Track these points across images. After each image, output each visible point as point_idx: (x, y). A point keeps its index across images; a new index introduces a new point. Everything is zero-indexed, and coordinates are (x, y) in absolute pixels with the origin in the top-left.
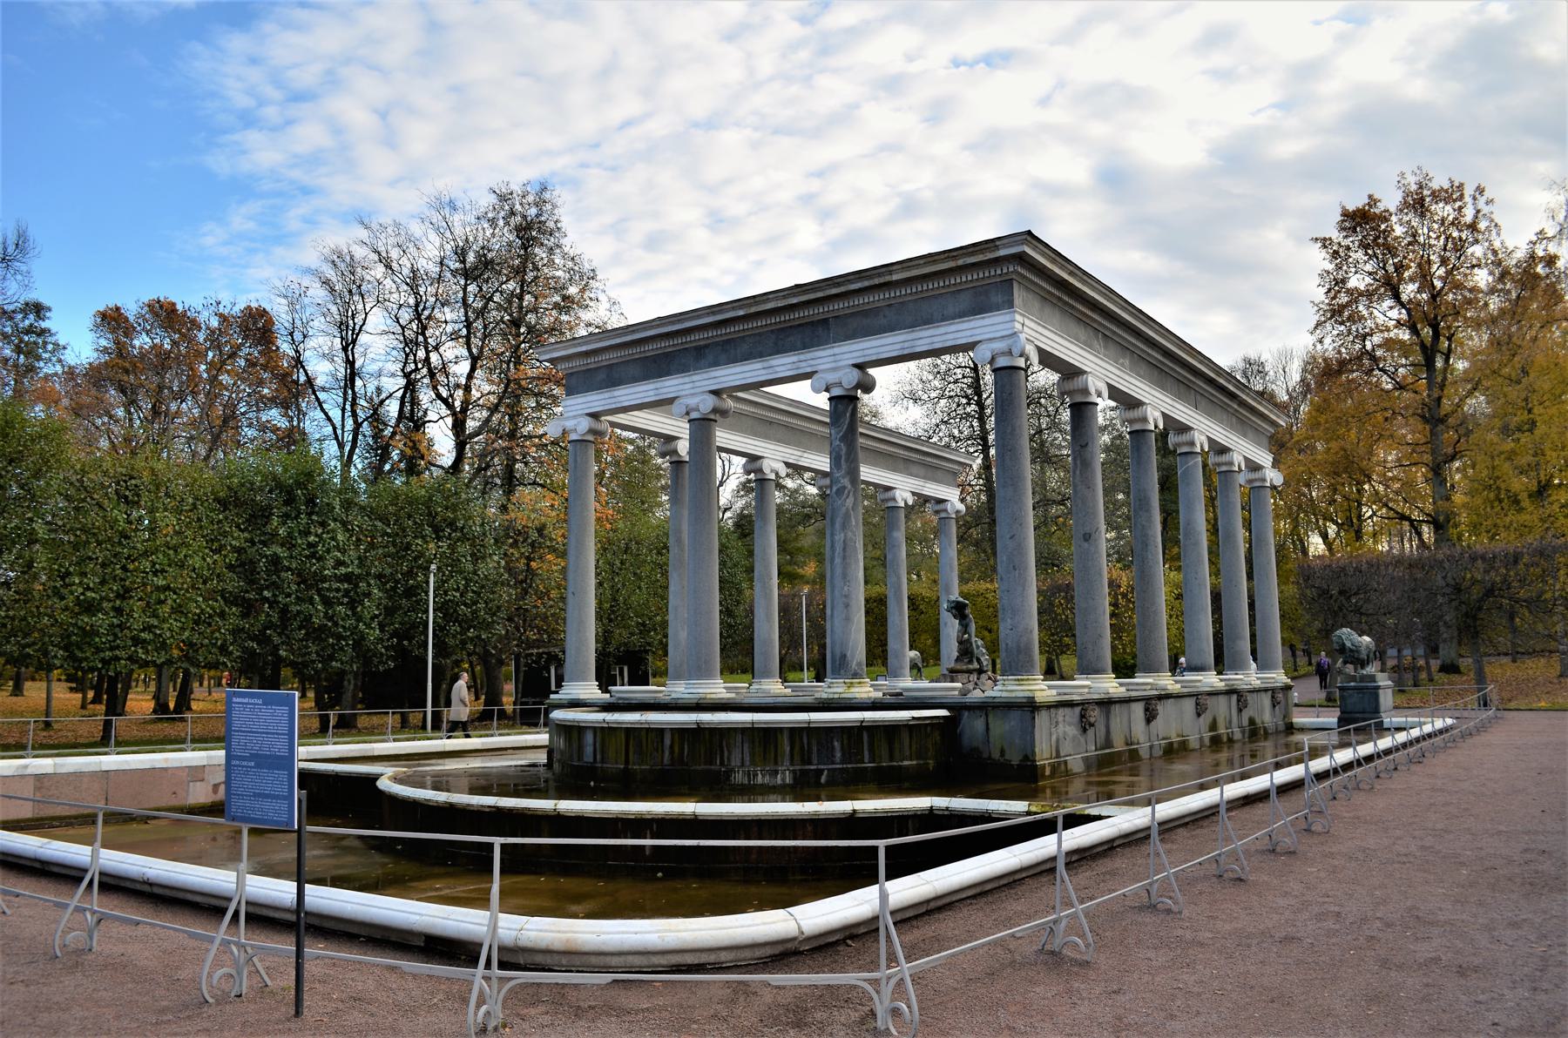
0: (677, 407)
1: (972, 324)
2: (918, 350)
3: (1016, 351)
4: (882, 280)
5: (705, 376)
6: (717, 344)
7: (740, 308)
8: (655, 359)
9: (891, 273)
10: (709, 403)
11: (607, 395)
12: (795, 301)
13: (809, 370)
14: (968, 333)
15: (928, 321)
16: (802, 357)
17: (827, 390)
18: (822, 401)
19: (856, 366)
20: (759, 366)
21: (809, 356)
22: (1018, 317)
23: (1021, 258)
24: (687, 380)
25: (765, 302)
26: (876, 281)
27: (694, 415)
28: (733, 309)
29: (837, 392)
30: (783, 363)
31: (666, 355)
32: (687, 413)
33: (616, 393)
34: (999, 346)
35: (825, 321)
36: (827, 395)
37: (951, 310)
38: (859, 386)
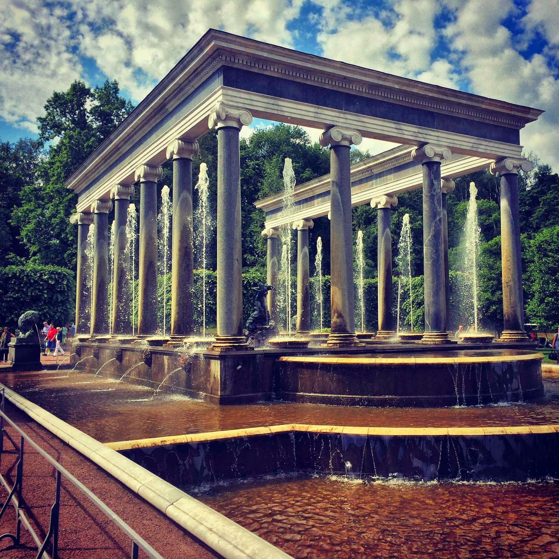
1: (504, 147)
2: (480, 150)
7: (398, 83)
9: (482, 103)
11: (272, 101)
12: (431, 94)
13: (423, 140)
16: (421, 131)
20: (393, 125)
24: (342, 115)
25: (414, 87)
28: (394, 82)
35: (432, 114)
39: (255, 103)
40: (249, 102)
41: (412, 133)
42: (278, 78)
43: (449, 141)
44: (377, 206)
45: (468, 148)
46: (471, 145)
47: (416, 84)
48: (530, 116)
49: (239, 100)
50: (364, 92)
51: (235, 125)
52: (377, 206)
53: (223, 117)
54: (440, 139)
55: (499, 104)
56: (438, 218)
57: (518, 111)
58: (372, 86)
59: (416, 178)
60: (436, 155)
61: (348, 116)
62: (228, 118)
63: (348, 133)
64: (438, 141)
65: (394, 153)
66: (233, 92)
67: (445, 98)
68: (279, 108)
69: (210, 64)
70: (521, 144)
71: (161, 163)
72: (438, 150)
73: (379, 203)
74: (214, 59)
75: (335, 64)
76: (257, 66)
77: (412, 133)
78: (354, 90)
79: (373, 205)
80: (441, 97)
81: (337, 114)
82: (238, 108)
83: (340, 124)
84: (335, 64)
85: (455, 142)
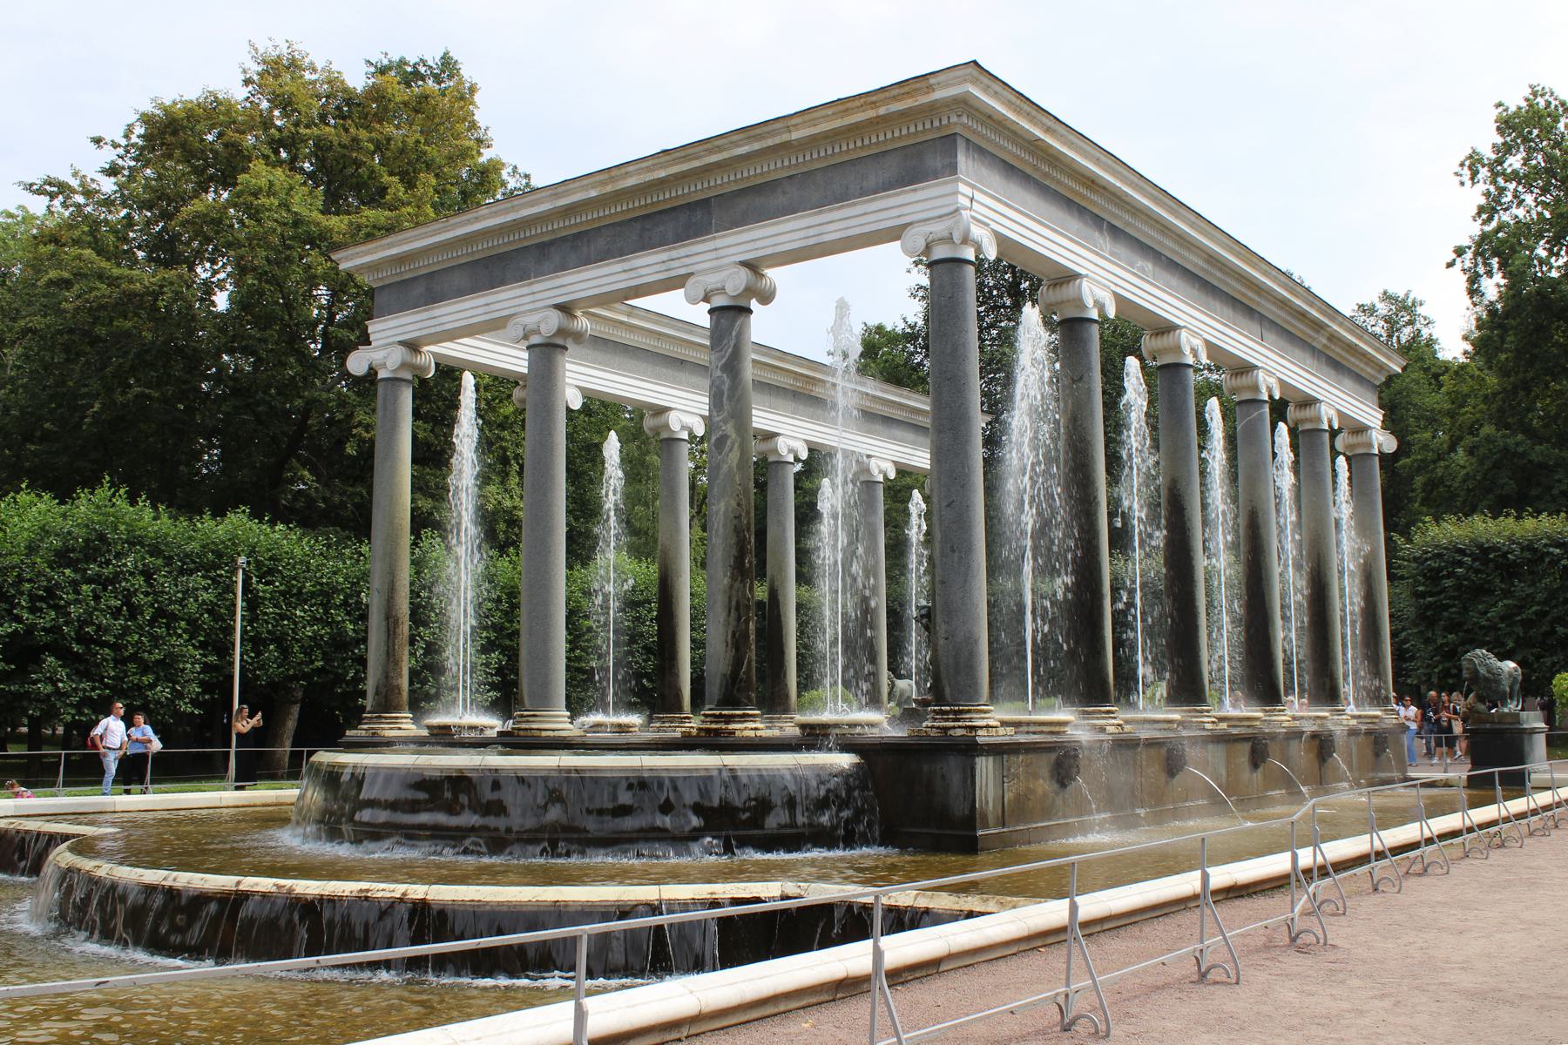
0: (515, 330)
3: (957, 237)
4: (777, 140)
6: (564, 239)
7: (593, 186)
10: (554, 320)
12: (662, 174)
13: (683, 271)
15: (842, 197)
16: (674, 254)
17: (706, 299)
18: (700, 315)
19: (744, 264)
20: (617, 267)
21: (683, 252)
22: (962, 188)
23: (964, 104)
26: (770, 142)
27: (535, 340)
28: (585, 188)
29: (719, 301)
30: (649, 264)
31: (500, 257)
32: (526, 337)
33: (437, 312)
34: (939, 229)
35: (705, 203)
36: (708, 307)
37: (872, 181)
38: (750, 292)
41: (657, 268)
47: (623, 170)
50: (561, 227)
55: (830, 112)
57: (895, 98)
61: (536, 287)
77: (657, 268)
80: (685, 167)
83: (522, 309)
85: (759, 244)
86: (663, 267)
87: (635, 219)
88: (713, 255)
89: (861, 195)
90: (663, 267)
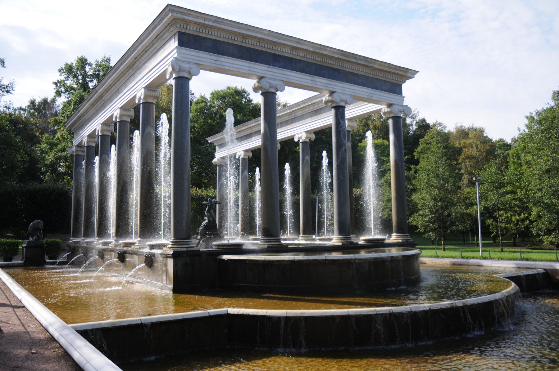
2: (374, 98)
5: (281, 72)
6: (286, 57)
8: (248, 49)
9: (374, 63)
11: (215, 58)
13: (332, 89)
14: (390, 99)
16: (330, 82)
35: (338, 70)
39: (201, 59)
40: (197, 58)
41: (323, 84)
42: (220, 41)
43: (351, 90)
44: (299, 141)
45: (365, 97)
46: (367, 94)
48: (409, 75)
49: (190, 57)
50: (287, 53)
51: (186, 75)
52: (299, 141)
53: (177, 69)
54: (344, 89)
56: (344, 148)
57: (400, 70)
58: (294, 48)
59: (327, 119)
60: (341, 100)
62: (180, 70)
63: (274, 83)
64: (343, 89)
65: (312, 100)
66: (185, 50)
67: (347, 59)
68: (221, 63)
69: (168, 30)
70: (403, 95)
71: (132, 107)
72: (344, 97)
73: (301, 138)
74: (172, 26)
75: (264, 32)
76: (204, 31)
77: (323, 84)
78: (278, 51)
79: (296, 140)
80: (344, 58)
81: (267, 69)
82: (189, 63)
84: (264, 32)
86: (325, 85)
87: (314, 64)
88: (341, 88)
89: (381, 90)
90: (325, 85)
